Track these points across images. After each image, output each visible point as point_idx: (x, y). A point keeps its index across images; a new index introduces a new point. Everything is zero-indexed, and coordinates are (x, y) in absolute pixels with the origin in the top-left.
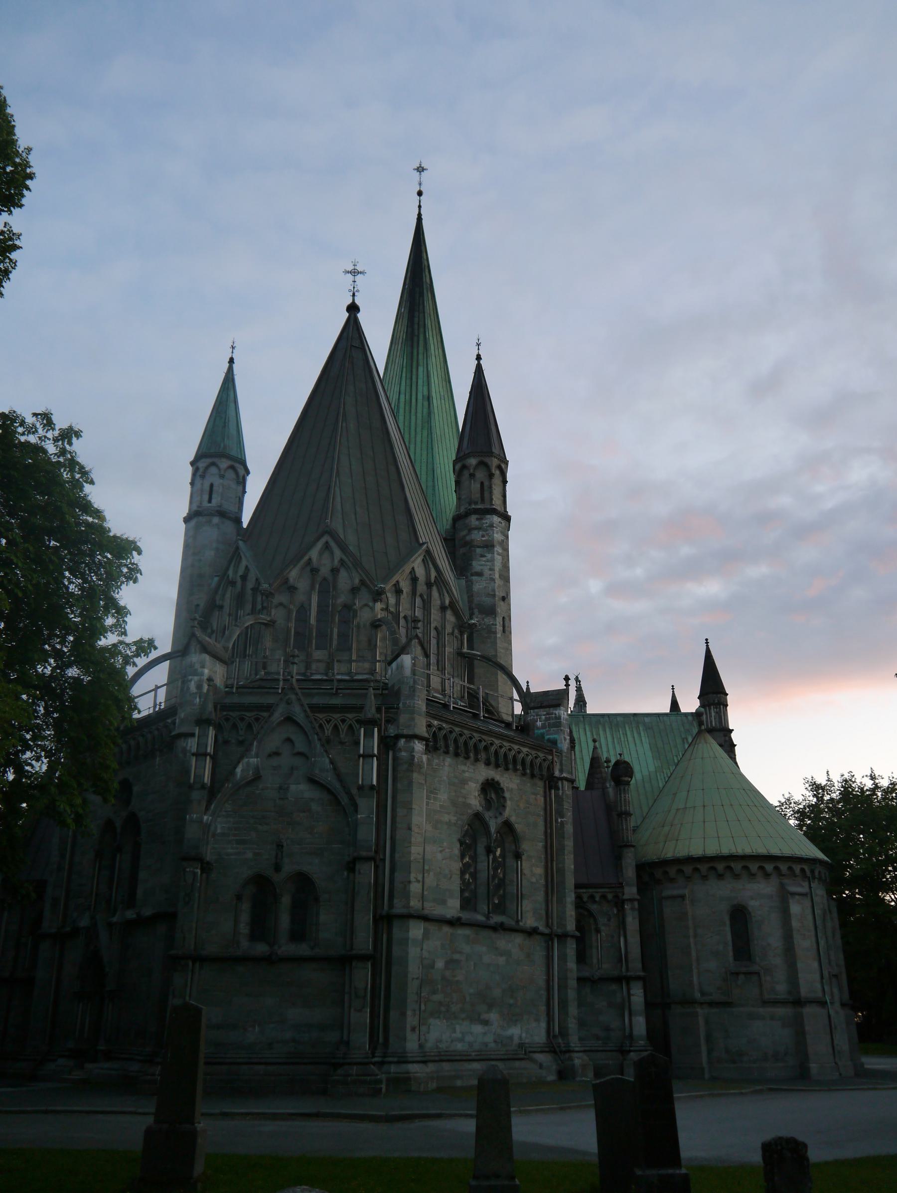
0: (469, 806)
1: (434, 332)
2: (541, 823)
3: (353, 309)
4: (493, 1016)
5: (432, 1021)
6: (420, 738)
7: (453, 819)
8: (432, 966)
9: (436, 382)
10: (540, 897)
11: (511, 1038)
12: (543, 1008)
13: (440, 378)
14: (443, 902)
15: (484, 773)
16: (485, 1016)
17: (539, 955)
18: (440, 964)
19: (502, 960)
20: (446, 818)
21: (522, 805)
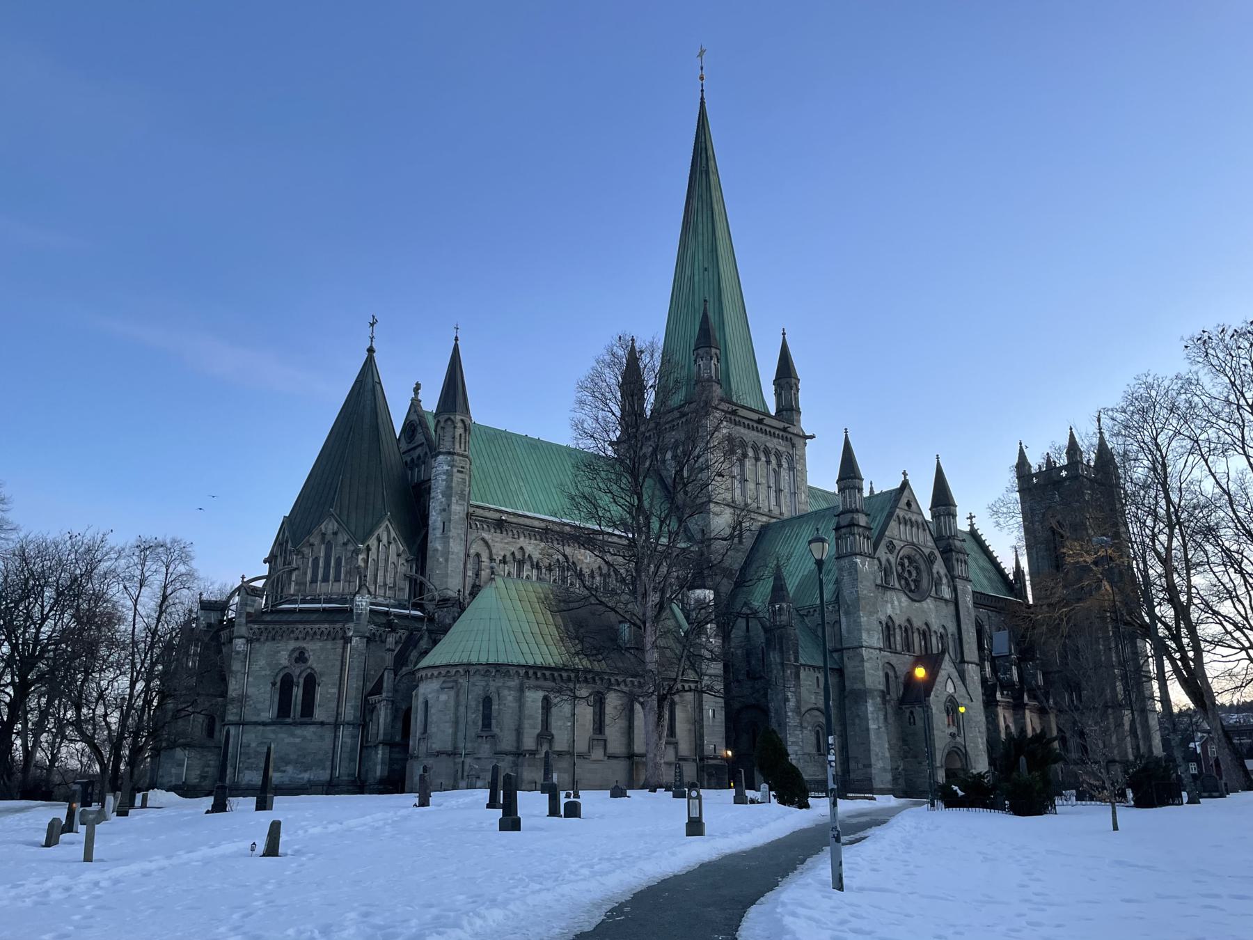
0: (281, 664)
1: (705, 210)
2: (338, 663)
3: (371, 350)
4: (290, 769)
5: (246, 772)
6: (242, 637)
7: (268, 672)
8: (249, 746)
9: (701, 258)
10: (334, 705)
11: (303, 778)
12: (329, 764)
13: (706, 251)
14: (259, 715)
15: (292, 645)
16: (284, 769)
17: (328, 734)
18: (253, 745)
19: (298, 740)
20: (263, 673)
21: (322, 657)
